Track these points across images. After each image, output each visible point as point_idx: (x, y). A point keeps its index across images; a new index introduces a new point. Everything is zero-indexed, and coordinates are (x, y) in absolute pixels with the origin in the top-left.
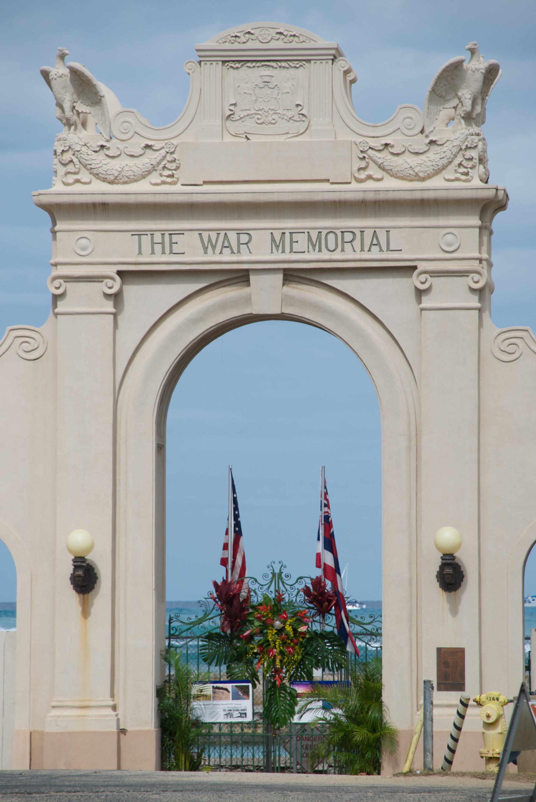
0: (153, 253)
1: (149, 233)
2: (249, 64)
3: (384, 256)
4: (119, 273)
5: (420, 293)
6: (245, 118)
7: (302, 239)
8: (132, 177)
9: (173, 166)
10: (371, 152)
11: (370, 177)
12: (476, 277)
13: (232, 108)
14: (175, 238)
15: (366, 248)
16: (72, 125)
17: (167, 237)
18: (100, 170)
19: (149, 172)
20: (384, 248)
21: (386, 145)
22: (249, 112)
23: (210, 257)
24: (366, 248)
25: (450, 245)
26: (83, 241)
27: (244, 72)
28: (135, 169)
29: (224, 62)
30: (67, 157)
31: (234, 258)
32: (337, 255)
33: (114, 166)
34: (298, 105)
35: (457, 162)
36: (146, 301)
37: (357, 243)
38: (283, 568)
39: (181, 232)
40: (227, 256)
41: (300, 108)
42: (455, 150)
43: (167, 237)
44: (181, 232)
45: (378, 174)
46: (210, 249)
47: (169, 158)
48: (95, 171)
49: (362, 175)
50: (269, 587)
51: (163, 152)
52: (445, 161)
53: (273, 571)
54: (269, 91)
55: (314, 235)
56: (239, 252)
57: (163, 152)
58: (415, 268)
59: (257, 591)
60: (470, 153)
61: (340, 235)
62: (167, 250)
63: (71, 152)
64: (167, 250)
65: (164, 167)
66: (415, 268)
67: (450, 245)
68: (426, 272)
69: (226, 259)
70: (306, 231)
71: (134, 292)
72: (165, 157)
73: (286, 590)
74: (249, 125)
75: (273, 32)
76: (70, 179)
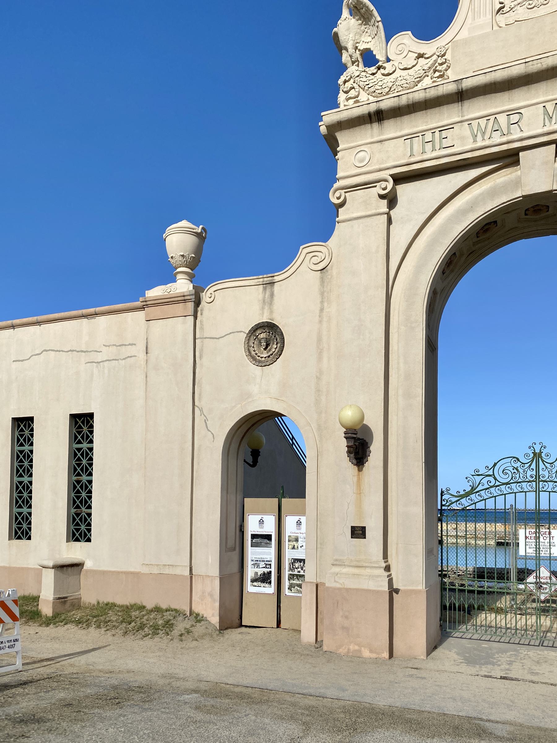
6: (516, 8)
36: (418, 198)
38: (543, 448)
47: (440, 61)
50: (530, 465)
53: (534, 450)
59: (519, 468)
71: (405, 191)
73: (546, 467)
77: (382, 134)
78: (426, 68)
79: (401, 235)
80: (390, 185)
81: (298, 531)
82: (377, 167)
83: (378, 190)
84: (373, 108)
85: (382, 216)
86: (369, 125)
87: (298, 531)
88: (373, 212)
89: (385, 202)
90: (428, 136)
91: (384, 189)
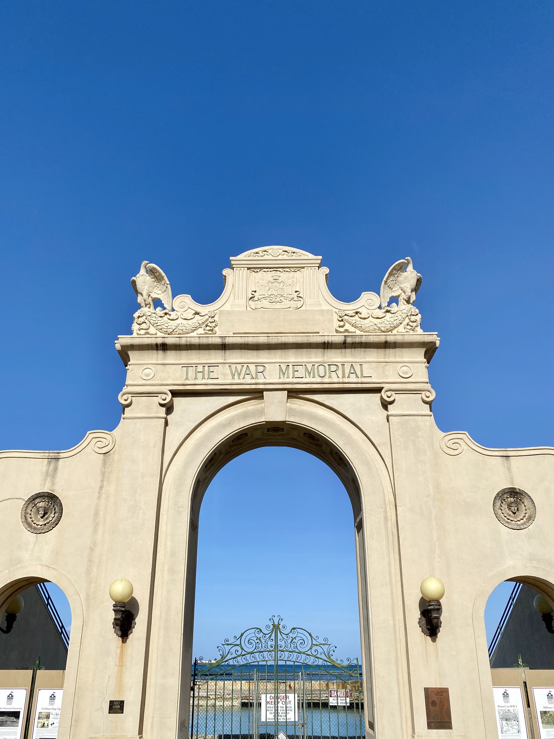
0: (196, 378)
1: (194, 365)
2: (265, 270)
3: (360, 380)
4: (170, 391)
5: (385, 405)
7: (301, 369)
8: (185, 330)
9: (214, 324)
10: (346, 317)
11: (346, 331)
12: (428, 394)
13: (253, 293)
14: (212, 369)
15: (347, 376)
16: (148, 304)
17: (206, 368)
18: (163, 326)
19: (196, 329)
20: (359, 376)
21: (357, 313)
22: (264, 296)
23: (236, 381)
24: (347, 376)
25: (406, 373)
26: (147, 371)
27: (261, 274)
28: (187, 326)
29: (248, 269)
30: (141, 320)
31: (254, 381)
32: (326, 380)
33: (173, 324)
34: (296, 292)
35: (405, 323)
36: (188, 410)
37: (340, 373)
39: (216, 365)
40: (248, 380)
41: (298, 293)
42: (404, 316)
43: (206, 368)
44: (216, 365)
45: (352, 329)
46: (236, 376)
47: (210, 320)
48: (160, 327)
49: (342, 330)
51: (207, 317)
52: (398, 322)
54: (277, 285)
55: (309, 367)
56: (257, 377)
57: (207, 317)
58: (383, 388)
60: (413, 318)
61: (327, 367)
62: (206, 377)
63: (144, 317)
64: (206, 377)
65: (207, 326)
66: (383, 388)
67: (406, 373)
68: (390, 390)
69: (247, 382)
70: (303, 364)
72: (207, 320)
74: (265, 303)
75: (281, 251)
76: (143, 332)
77: (165, 359)
78: (200, 322)
79: (175, 435)
80: (169, 397)
81: (51, 707)
82: (159, 382)
83: (159, 399)
84: (160, 341)
85: (161, 419)
86: (156, 351)
87: (51, 707)
88: (154, 415)
89: (164, 409)
90: (200, 368)
91: (164, 400)
